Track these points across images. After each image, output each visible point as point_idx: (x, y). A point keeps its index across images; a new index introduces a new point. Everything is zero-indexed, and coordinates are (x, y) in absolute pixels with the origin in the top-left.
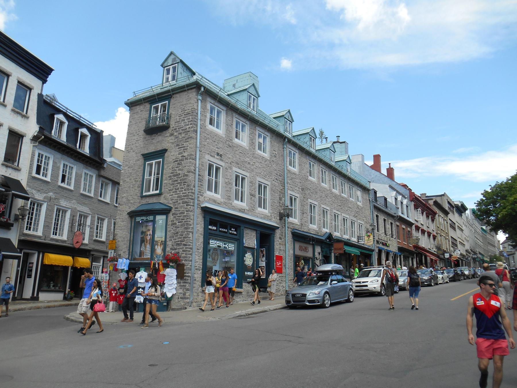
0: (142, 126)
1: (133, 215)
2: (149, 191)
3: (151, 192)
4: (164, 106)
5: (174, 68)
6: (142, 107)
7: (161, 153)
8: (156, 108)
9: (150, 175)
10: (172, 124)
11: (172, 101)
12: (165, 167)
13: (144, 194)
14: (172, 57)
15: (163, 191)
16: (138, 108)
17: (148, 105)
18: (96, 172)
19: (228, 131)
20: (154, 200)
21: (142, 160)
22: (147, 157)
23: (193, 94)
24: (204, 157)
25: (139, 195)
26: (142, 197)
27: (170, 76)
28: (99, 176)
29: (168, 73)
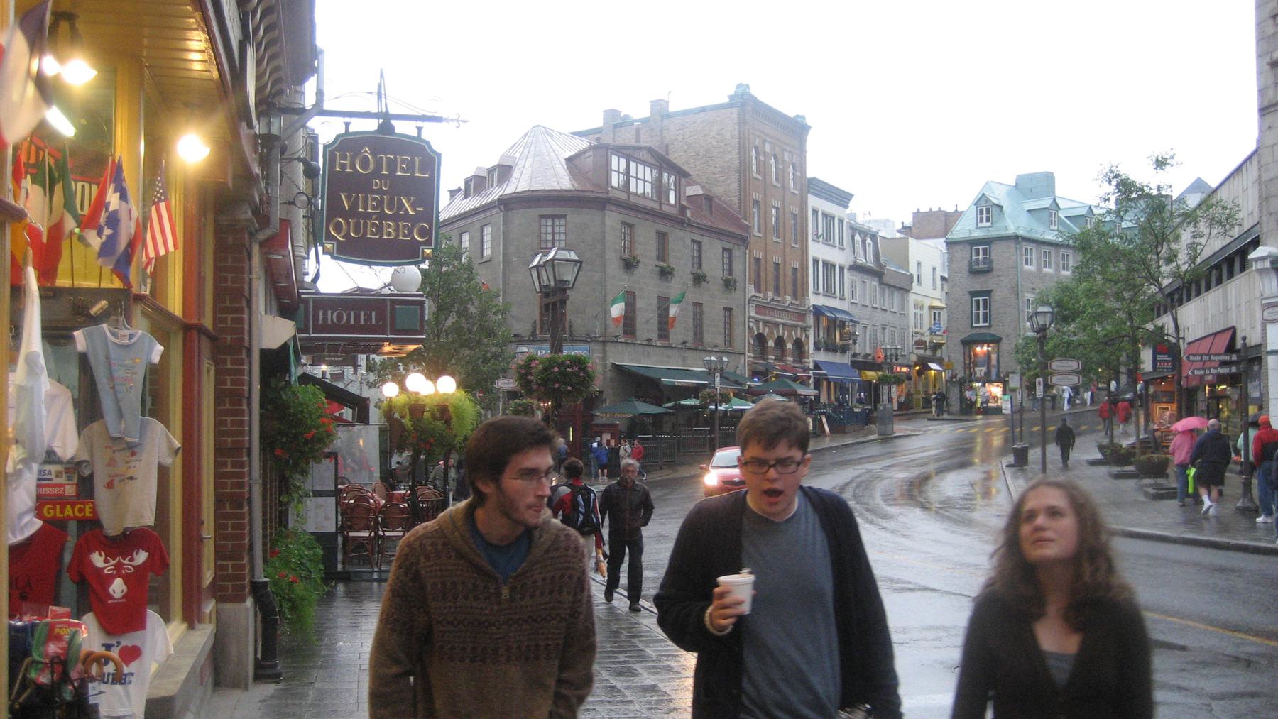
0: (965, 264)
1: (969, 343)
2: (978, 322)
3: (981, 324)
4: (985, 251)
5: (988, 211)
6: (961, 247)
7: (988, 293)
8: (977, 251)
9: (978, 308)
10: (995, 265)
11: (993, 247)
12: (992, 304)
13: (974, 325)
14: (984, 199)
15: (992, 323)
16: (957, 248)
17: (968, 247)
18: (877, 279)
19: (1039, 265)
20: (985, 331)
21: (968, 297)
22: (973, 294)
23: (1012, 244)
24: (1023, 296)
25: (969, 325)
26: (972, 327)
27: (984, 216)
28: (881, 283)
29: (982, 212)
